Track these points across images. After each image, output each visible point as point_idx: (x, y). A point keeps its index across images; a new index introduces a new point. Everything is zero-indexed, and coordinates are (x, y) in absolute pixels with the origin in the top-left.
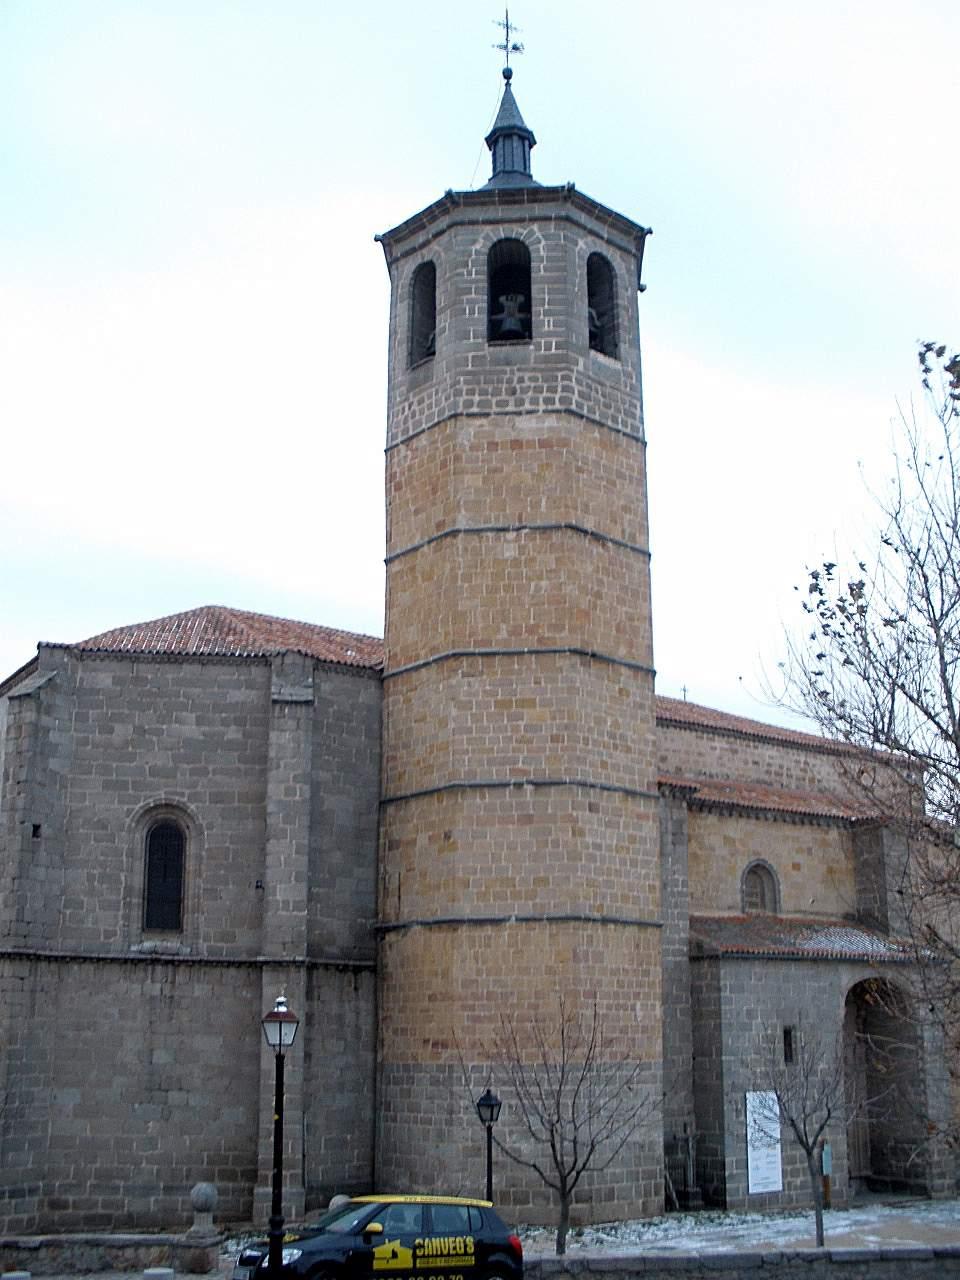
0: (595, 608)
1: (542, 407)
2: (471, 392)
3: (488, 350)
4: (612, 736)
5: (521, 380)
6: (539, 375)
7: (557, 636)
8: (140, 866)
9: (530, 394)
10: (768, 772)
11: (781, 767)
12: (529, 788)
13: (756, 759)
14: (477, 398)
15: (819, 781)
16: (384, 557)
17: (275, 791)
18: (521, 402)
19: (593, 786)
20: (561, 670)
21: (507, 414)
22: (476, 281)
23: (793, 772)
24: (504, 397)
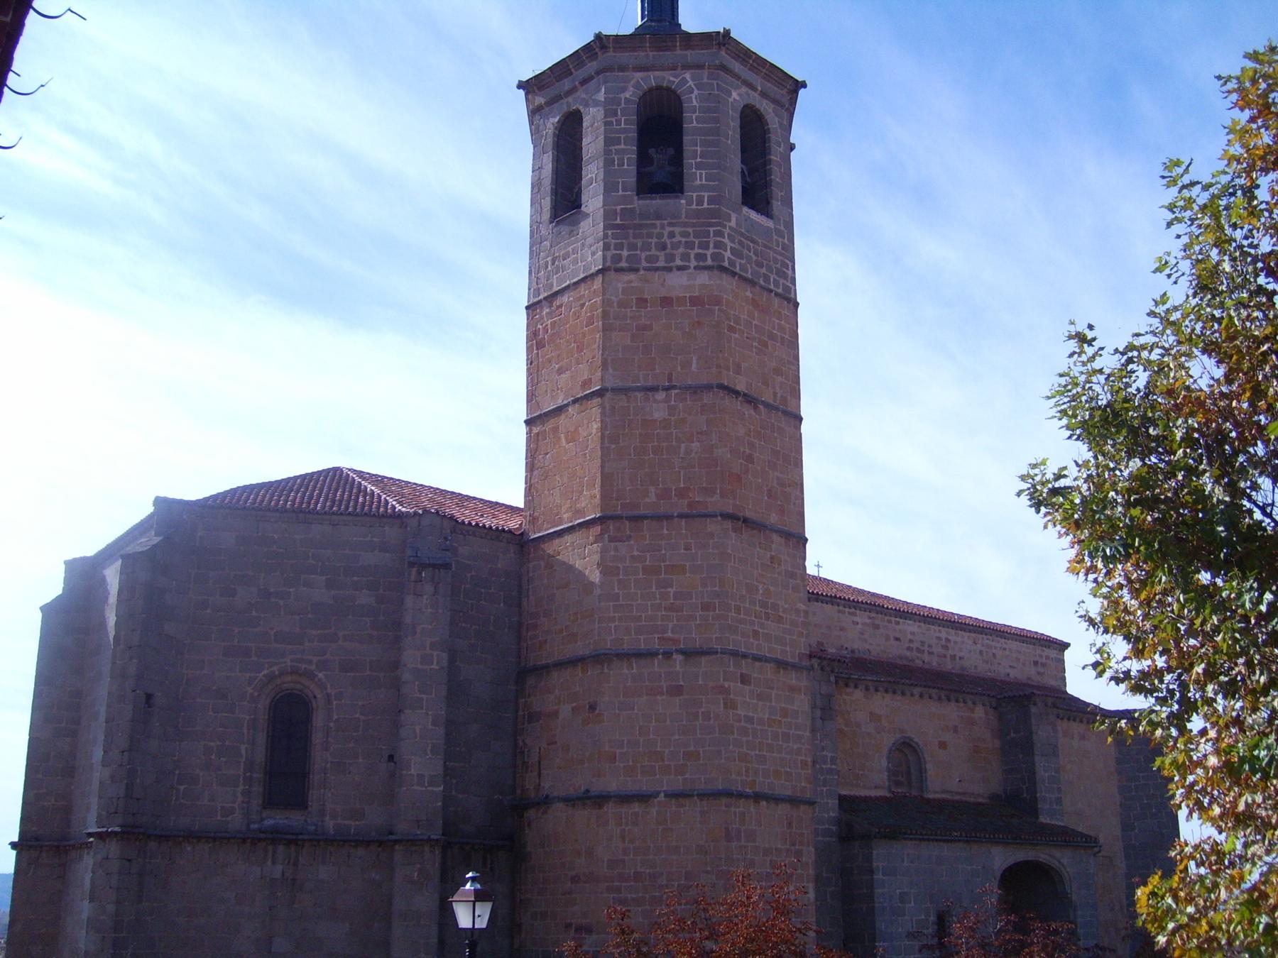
0: (747, 471)
1: (693, 263)
2: (619, 247)
3: (638, 204)
4: (764, 605)
5: (672, 235)
6: (690, 230)
7: (709, 499)
8: (262, 738)
9: (681, 250)
10: (909, 648)
12: (678, 658)
13: (898, 636)
15: (960, 658)
16: (525, 418)
17: (411, 658)
18: (670, 258)
19: (745, 656)
20: (712, 535)
21: (657, 269)
22: (625, 131)
23: (934, 650)
24: (654, 252)
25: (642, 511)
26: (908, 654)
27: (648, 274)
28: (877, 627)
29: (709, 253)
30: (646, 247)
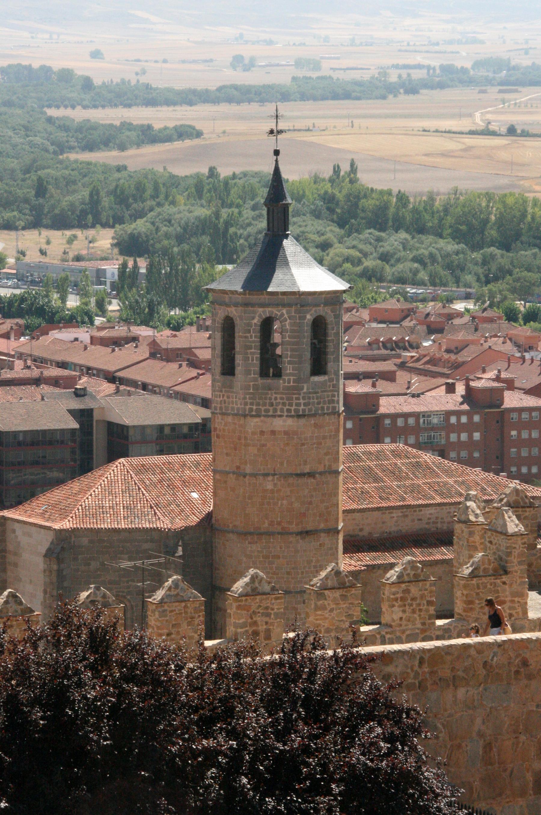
1: (285, 414)
2: (252, 404)
3: (261, 381)
5: (276, 399)
10: (428, 523)
11: (437, 518)
14: (254, 407)
18: (275, 410)
24: (267, 407)
25: (262, 530)
26: (427, 526)
27: (266, 419)
28: (407, 516)
29: (293, 408)
30: (264, 404)
